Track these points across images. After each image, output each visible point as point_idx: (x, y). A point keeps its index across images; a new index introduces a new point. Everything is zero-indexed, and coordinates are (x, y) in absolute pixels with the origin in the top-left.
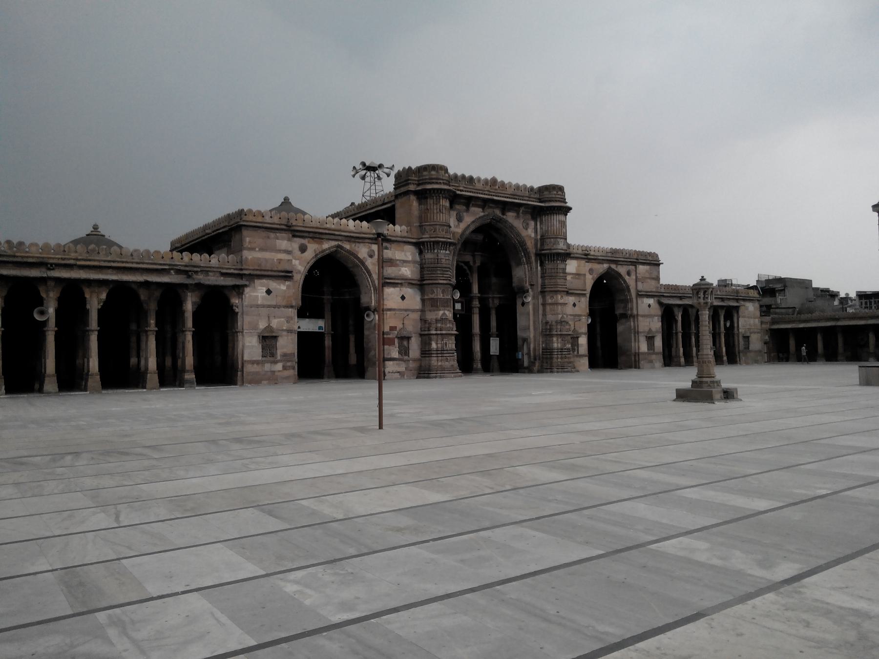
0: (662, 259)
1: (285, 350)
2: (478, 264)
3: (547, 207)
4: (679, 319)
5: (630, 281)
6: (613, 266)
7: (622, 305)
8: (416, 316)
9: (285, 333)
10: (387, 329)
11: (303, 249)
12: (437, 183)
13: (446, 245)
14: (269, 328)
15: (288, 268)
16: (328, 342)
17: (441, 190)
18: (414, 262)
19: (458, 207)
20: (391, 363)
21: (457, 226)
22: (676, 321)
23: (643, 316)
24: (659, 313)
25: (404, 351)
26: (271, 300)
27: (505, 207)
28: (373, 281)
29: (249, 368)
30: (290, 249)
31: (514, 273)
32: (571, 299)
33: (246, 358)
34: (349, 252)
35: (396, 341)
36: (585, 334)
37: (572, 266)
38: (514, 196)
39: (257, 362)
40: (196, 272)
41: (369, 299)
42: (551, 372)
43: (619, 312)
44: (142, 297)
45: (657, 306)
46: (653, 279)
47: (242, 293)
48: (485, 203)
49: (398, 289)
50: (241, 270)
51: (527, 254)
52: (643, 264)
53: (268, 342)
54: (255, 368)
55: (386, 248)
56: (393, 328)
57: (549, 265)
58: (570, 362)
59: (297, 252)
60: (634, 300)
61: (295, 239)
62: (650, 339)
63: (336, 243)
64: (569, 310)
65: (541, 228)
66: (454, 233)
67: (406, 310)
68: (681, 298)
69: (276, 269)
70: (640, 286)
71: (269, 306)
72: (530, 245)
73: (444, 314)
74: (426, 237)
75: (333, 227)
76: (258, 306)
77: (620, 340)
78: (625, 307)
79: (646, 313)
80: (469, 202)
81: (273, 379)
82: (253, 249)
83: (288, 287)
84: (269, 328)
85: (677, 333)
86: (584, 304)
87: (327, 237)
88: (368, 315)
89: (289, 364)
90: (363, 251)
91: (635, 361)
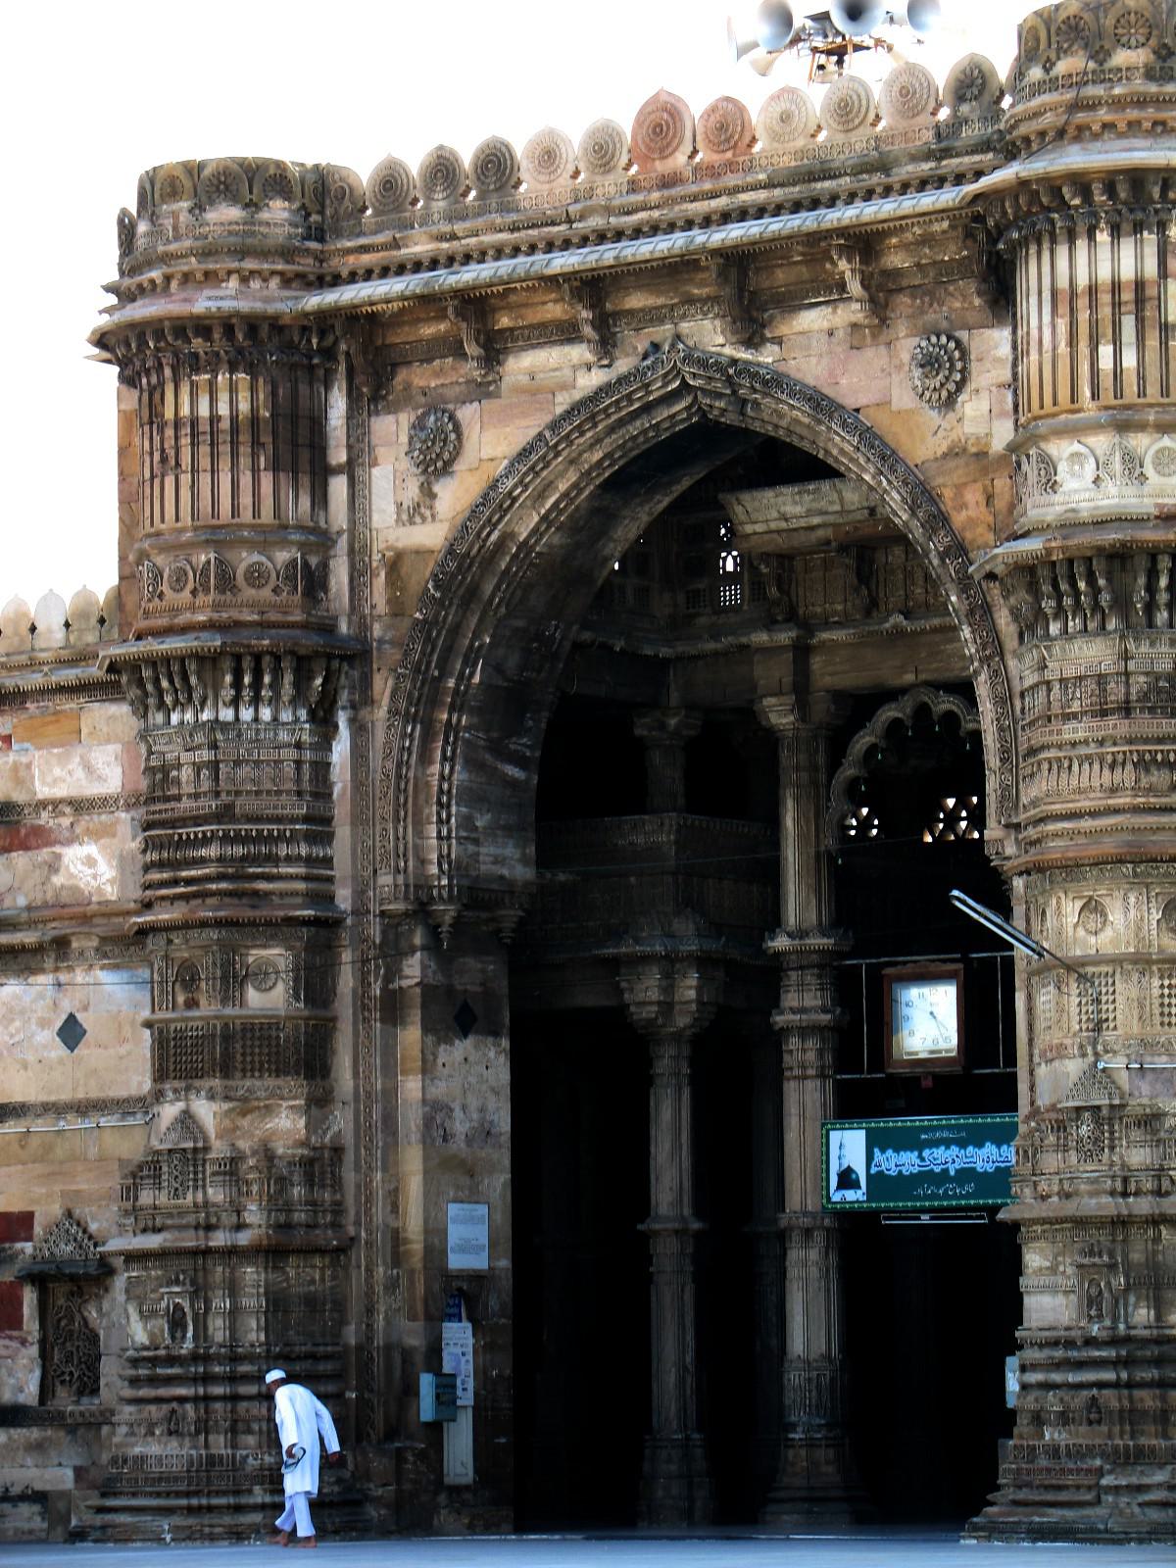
18: (133, 801)
19: (419, 377)
21: (413, 514)
35: (29, 1297)
66: (395, 563)
73: (187, 1119)
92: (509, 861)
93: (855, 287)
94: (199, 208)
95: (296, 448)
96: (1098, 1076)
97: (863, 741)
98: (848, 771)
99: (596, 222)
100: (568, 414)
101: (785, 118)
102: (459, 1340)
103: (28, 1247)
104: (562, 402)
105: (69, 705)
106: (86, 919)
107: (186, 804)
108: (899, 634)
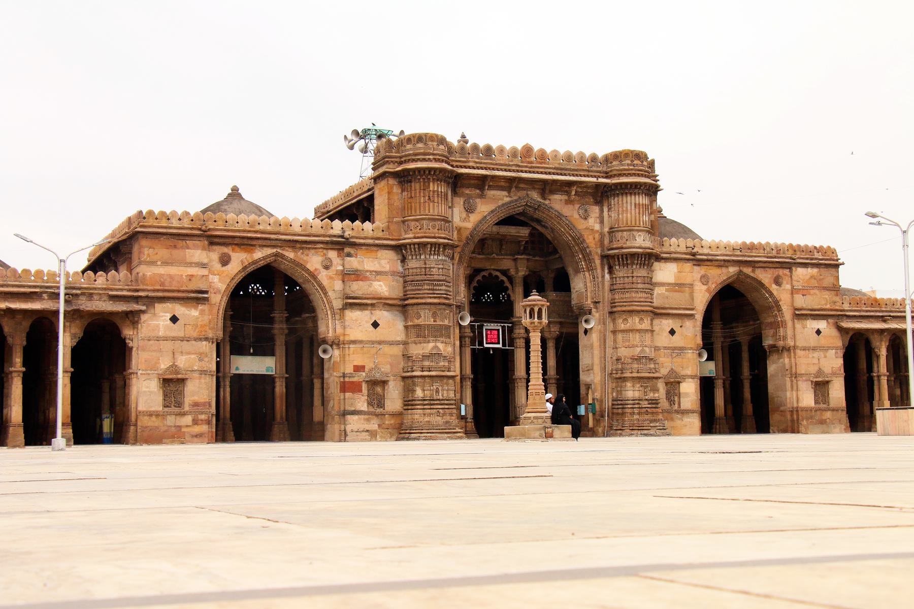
0: (842, 257)
1: (196, 398)
2: (522, 272)
3: (616, 185)
4: (883, 352)
5: (782, 293)
6: (748, 270)
7: (771, 332)
8: (397, 350)
9: (196, 375)
10: (349, 369)
11: (225, 261)
12: (424, 160)
13: (436, 248)
14: (174, 368)
15: (203, 287)
16: (280, 388)
17: (430, 169)
18: (393, 273)
19: (467, 191)
20: (356, 417)
22: (878, 357)
23: (804, 349)
24: (839, 343)
25: (376, 401)
26: (177, 330)
27: (546, 188)
28: (330, 302)
29: (144, 421)
30: (205, 261)
31: (572, 286)
33: (140, 408)
34: (293, 261)
36: (693, 377)
37: (665, 273)
38: (561, 171)
39: (157, 415)
40: (77, 295)
41: (328, 328)
42: (621, 435)
43: (767, 342)
44: (6, 329)
45: (834, 332)
46: (825, 289)
47: (137, 322)
48: (511, 184)
49: (367, 312)
50: (137, 291)
51: (587, 257)
52: (805, 265)
53: (172, 387)
54: (153, 422)
55: (349, 255)
56: (358, 369)
57: (620, 272)
58: (655, 421)
59: (217, 266)
60: (790, 324)
61: (215, 247)
62: (821, 387)
63: (274, 250)
64: (663, 339)
65: (610, 216)
66: (459, 230)
67: (380, 343)
68: (883, 319)
69: (184, 288)
70: (801, 301)
71: (174, 339)
72: (591, 242)
73: (436, 347)
74: (408, 238)
75: (269, 228)
76: (158, 339)
77: (771, 387)
78: (775, 335)
79: (812, 344)
81: (176, 436)
82: (153, 263)
83: (202, 312)
84: (174, 368)
85: (879, 376)
86: (691, 332)
87: (260, 242)
88: (325, 351)
89: (203, 417)
90: (313, 261)
91: (793, 421)
93: (573, 193)
94: (438, 145)
96: (642, 351)
97: (479, 278)
98: (475, 284)
99: (514, 168)
100: (503, 205)
101: (556, 156)
103: (364, 374)
104: (500, 203)
105: (375, 249)
106: (380, 299)
107: (436, 277)
108: (494, 258)
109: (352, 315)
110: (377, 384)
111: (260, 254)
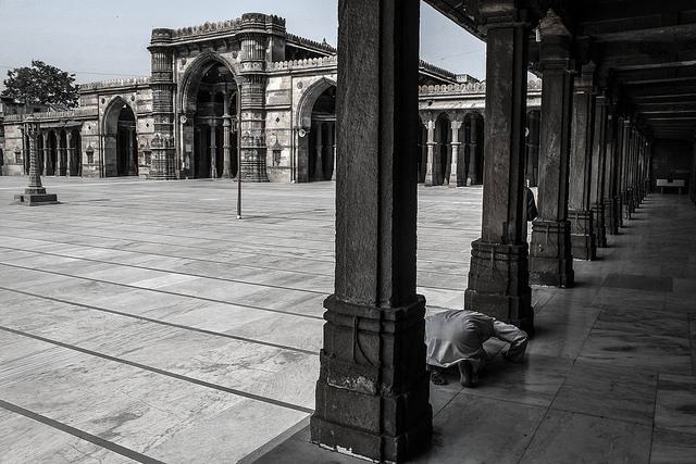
4: (430, 125)
11: (103, 101)
32: (275, 115)
37: (275, 84)
56: (142, 146)
72: (238, 71)
80: (187, 49)
92: (194, 108)
95: (169, 61)
102: (188, 160)
109: (140, 121)
110: (148, 153)
111: (113, 98)
